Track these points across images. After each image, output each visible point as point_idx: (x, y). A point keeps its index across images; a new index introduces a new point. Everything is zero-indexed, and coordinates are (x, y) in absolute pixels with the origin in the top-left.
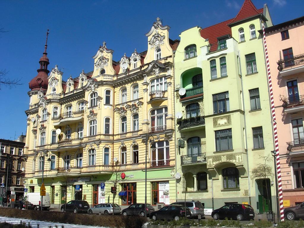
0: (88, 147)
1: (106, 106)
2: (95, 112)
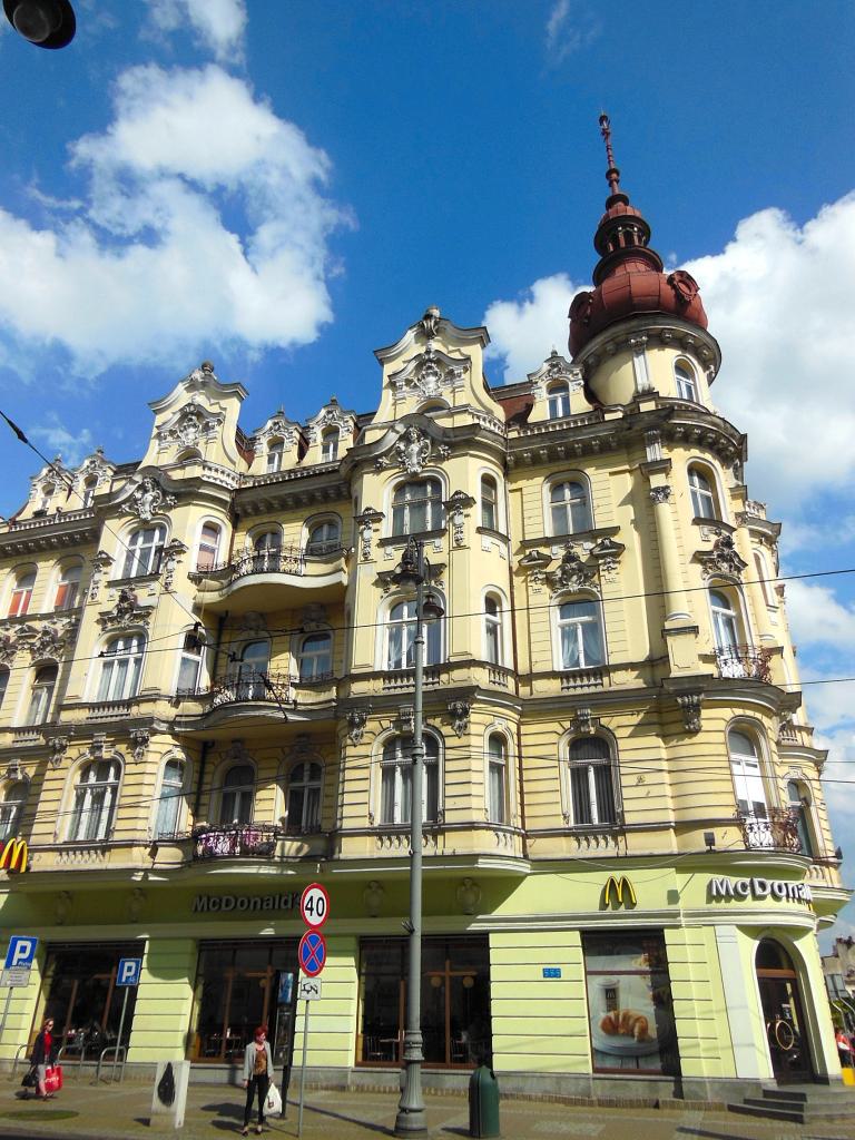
1: (488, 540)
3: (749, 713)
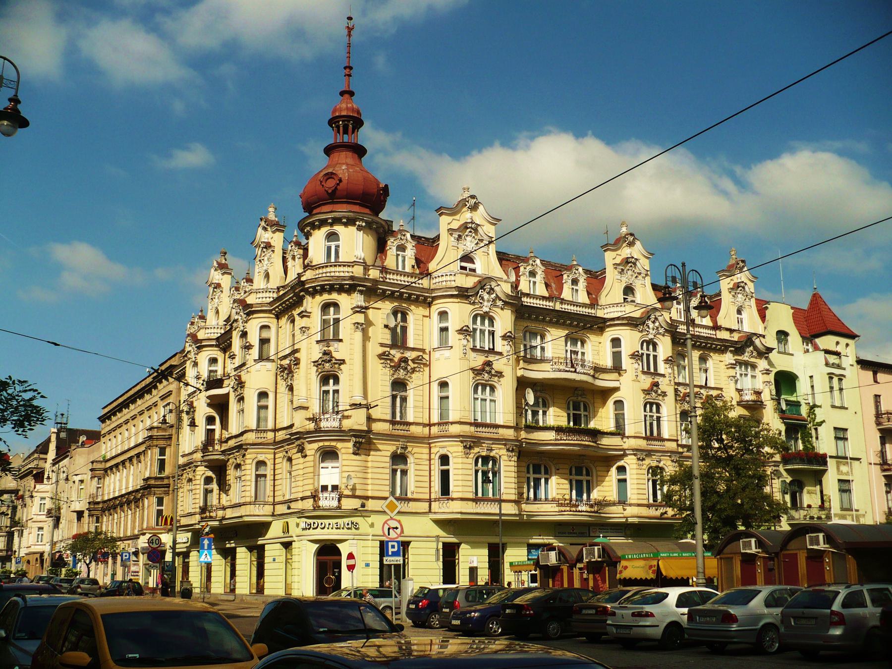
0: (252, 456)
2: (243, 379)
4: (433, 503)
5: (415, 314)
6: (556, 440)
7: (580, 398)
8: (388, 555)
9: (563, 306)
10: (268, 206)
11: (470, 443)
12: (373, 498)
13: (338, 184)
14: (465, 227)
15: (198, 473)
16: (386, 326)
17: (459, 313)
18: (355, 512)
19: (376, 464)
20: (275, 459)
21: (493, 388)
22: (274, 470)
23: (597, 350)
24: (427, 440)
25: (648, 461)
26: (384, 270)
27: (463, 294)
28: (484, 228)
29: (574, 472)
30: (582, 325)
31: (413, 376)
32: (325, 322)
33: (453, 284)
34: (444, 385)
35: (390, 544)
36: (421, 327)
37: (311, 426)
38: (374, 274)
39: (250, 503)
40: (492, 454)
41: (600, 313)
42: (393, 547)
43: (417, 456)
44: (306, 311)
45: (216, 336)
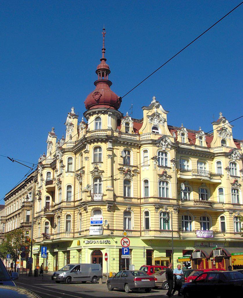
0: (65, 212)
1: (67, 174)
3: (96, 207)
4: (142, 232)
5: (134, 152)
6: (195, 205)
7: (204, 187)
8: (123, 254)
9: (196, 148)
10: (71, 108)
11: (158, 206)
12: (116, 230)
13: (100, 97)
14: (154, 115)
15: (42, 220)
16: (121, 157)
17: (152, 151)
18: (108, 236)
19: (117, 215)
20: (74, 214)
21: (167, 183)
22: (74, 218)
23: (211, 167)
24: (139, 205)
25: (234, 214)
26: (120, 133)
27: (154, 143)
28: (162, 115)
29: (202, 219)
30: (205, 156)
31: (133, 178)
32: (95, 155)
33: (150, 138)
34: (146, 181)
35: (124, 249)
36: (135, 157)
37: (90, 199)
38: (116, 134)
39: (64, 233)
40: (167, 211)
41: (212, 151)
42: (126, 250)
43: (135, 211)
44: (87, 150)
45: (50, 163)
